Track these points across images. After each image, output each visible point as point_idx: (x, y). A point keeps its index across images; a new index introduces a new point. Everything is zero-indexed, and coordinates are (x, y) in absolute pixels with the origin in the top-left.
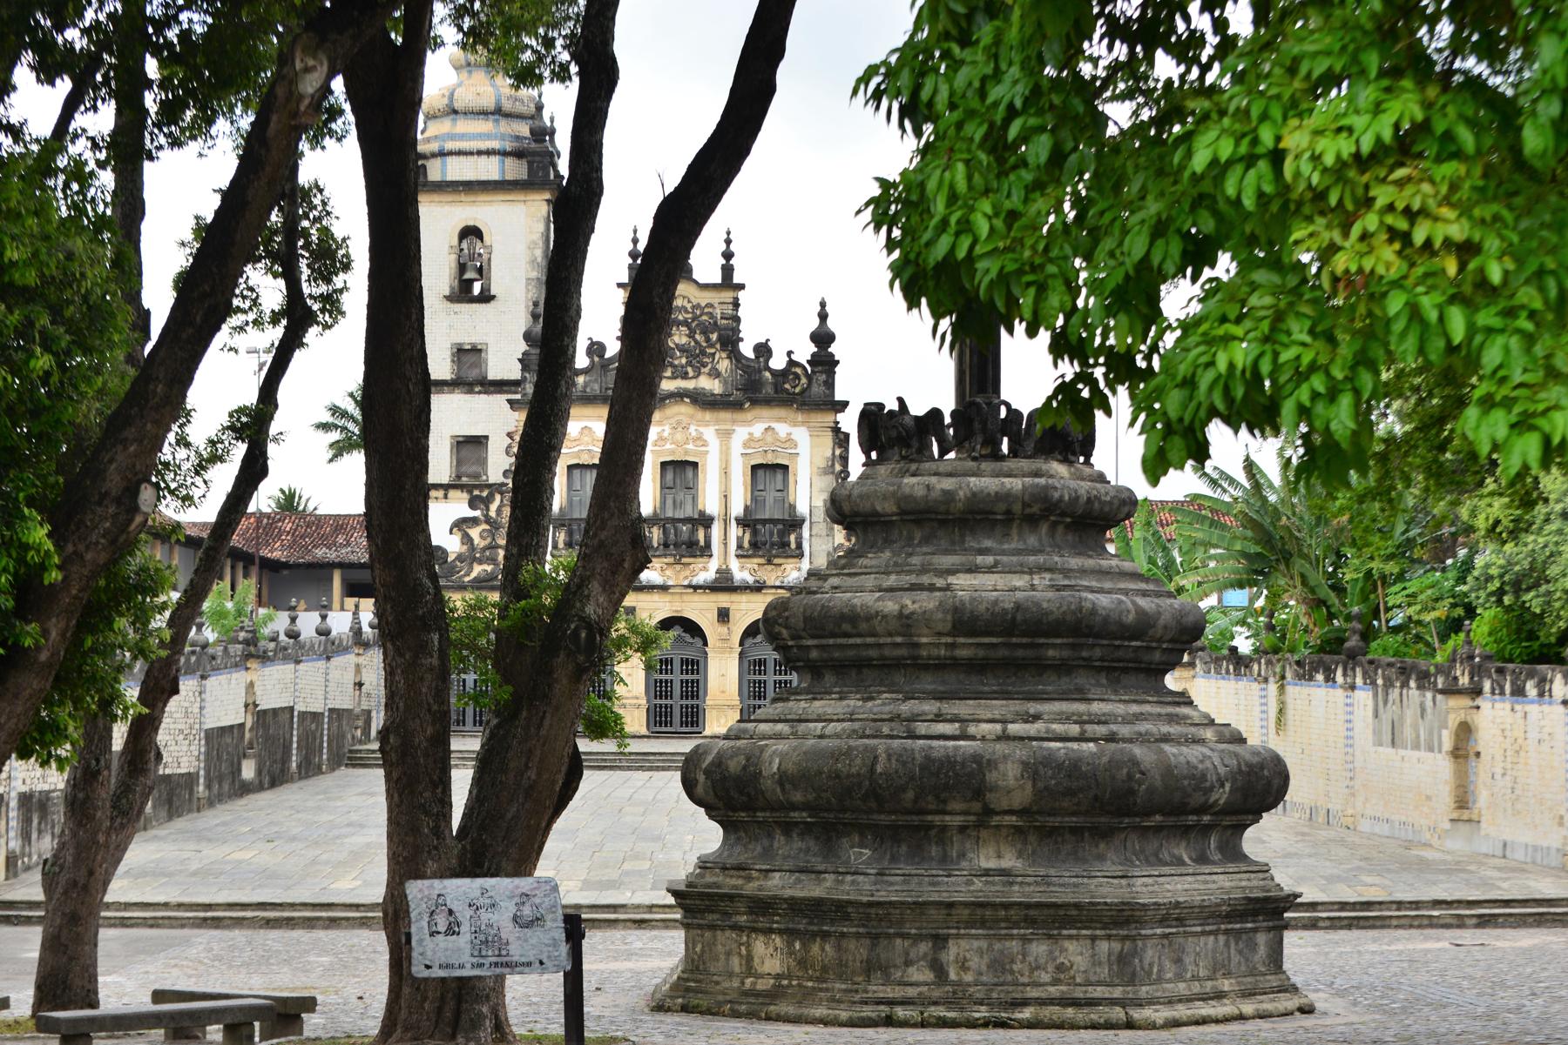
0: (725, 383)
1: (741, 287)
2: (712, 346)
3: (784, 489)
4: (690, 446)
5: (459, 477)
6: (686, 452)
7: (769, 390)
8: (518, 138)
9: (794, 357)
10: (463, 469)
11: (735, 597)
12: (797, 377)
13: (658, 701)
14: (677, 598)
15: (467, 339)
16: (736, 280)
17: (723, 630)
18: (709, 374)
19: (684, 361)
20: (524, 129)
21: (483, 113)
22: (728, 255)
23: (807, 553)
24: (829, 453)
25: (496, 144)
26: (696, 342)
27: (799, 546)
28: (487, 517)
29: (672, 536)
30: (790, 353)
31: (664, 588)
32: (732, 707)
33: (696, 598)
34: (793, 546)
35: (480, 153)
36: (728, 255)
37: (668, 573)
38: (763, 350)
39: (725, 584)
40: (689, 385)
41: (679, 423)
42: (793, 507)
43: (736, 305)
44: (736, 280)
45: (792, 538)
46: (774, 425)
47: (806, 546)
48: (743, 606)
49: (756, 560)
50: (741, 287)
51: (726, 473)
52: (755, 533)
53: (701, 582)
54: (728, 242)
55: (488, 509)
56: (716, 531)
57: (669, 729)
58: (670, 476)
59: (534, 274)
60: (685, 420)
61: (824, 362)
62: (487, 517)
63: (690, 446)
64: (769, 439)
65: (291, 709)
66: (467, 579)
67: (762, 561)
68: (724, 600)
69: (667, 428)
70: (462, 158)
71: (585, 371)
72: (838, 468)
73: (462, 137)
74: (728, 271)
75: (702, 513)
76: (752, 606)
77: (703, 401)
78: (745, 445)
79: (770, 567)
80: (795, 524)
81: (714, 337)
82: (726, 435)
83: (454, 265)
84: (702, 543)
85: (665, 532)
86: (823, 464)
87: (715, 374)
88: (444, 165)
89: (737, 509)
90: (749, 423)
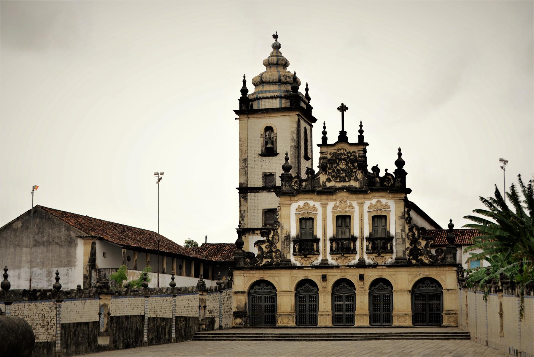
0: (360, 183)
1: (367, 144)
2: (355, 168)
3: (385, 226)
4: (347, 209)
5: (266, 225)
6: (346, 212)
7: (378, 185)
8: (287, 91)
9: (388, 172)
10: (268, 222)
11: (367, 270)
12: (389, 179)
13: (337, 313)
14: (343, 271)
15: (268, 170)
16: (365, 141)
17: (361, 283)
18: (354, 180)
19: (344, 175)
20: (289, 88)
21: (273, 83)
22: (361, 131)
23: (395, 251)
24: (403, 210)
25: (277, 94)
26: (349, 167)
27: (391, 248)
28: (268, 240)
29: (340, 246)
30: (386, 170)
31: (337, 267)
32: (365, 315)
33: (351, 270)
34: (389, 248)
35: (272, 98)
36: (361, 131)
37: (339, 261)
38: (376, 169)
39: (362, 264)
40: (347, 184)
41: (343, 200)
42: (389, 233)
43: (365, 151)
44: (365, 141)
45: (389, 245)
46: (380, 199)
47: (394, 248)
48: (369, 274)
49: (374, 255)
50: (367, 144)
51: (361, 219)
52: (373, 244)
53: (353, 264)
54: (361, 126)
55: (268, 237)
57: (341, 324)
58: (340, 221)
59: (293, 144)
60: (345, 198)
61: (401, 173)
62: (268, 240)
63: (347, 209)
64: (379, 205)
65: (143, 316)
66: (261, 265)
67: (376, 255)
68: (361, 271)
69: (338, 202)
70: (265, 100)
71: (305, 180)
72: (406, 216)
73: (265, 92)
74: (361, 138)
75: (353, 236)
76: (373, 273)
77: (352, 191)
78: (369, 208)
79: (379, 258)
80: (389, 239)
81: (356, 165)
82: (361, 204)
83: (262, 142)
84: (352, 248)
85: (338, 245)
86: (400, 214)
87: (357, 180)
88: (259, 103)
89: (366, 234)
90: (370, 199)
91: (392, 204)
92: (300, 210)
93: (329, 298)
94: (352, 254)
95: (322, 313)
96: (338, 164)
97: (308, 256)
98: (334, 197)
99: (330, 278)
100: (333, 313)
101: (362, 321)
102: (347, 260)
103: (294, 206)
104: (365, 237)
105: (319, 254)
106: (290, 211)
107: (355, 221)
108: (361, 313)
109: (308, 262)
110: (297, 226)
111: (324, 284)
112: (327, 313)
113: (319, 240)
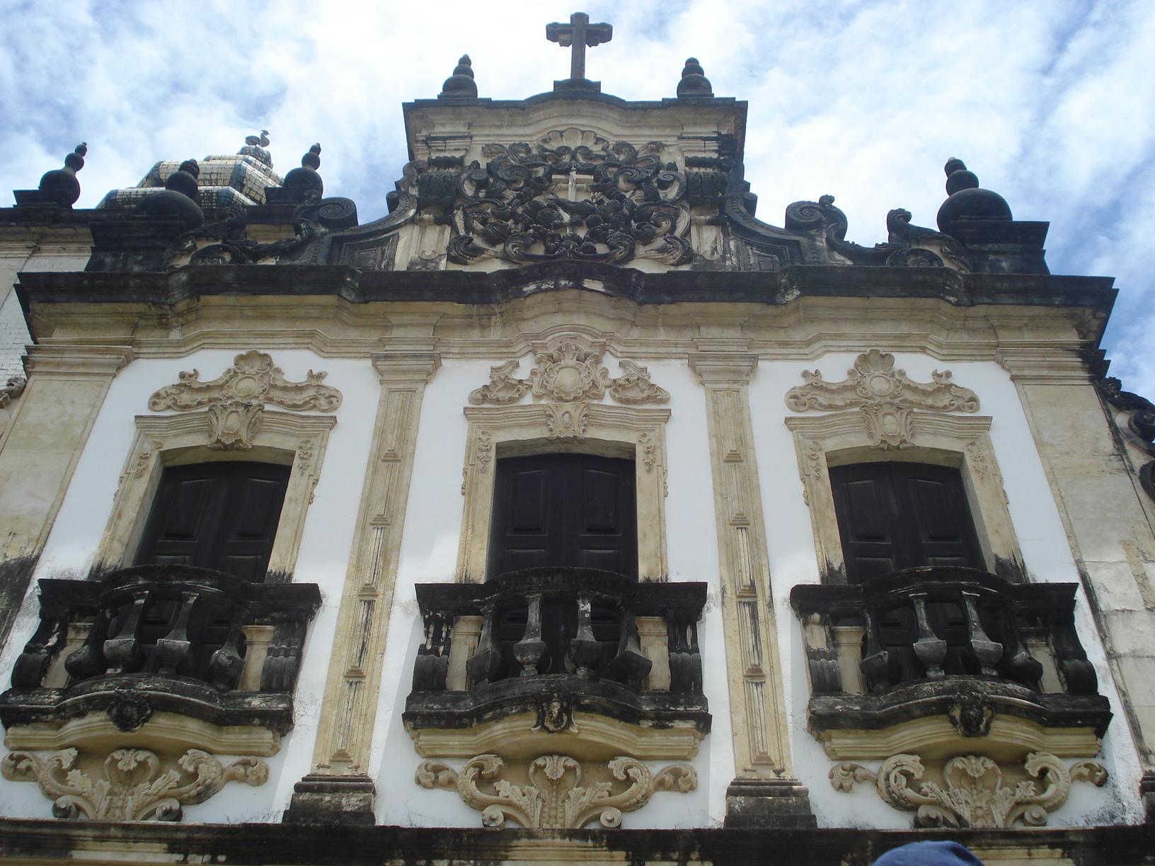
19: (582, 233)
37: (505, 788)
38: (819, 218)
42: (1013, 569)
47: (1105, 688)
56: (716, 639)
67: (935, 732)
80: (1052, 608)
84: (660, 676)
90: (805, 348)
91: (985, 381)
92: (186, 398)
94: (662, 721)
96: (542, 185)
97: (163, 727)
98: (495, 334)
102: (598, 790)
103: (150, 375)
104: (782, 593)
105: (282, 722)
106: (96, 406)
107: (674, 481)
109: (145, 790)
110: (121, 497)
113: (310, 597)
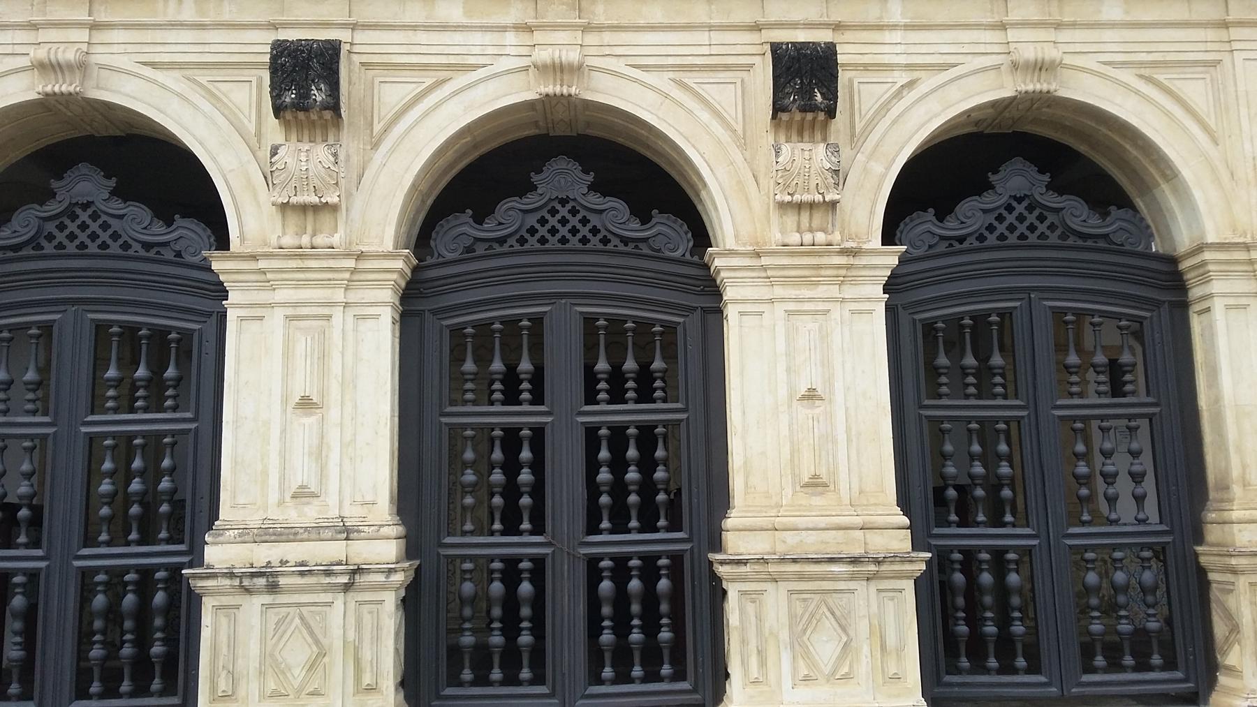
32: (866, 566)
93: (368, 352)
95: (263, 554)
99: (392, 94)
100: (413, 547)
101: (826, 646)
108: (811, 543)
111: (307, 158)
112: (333, 550)
